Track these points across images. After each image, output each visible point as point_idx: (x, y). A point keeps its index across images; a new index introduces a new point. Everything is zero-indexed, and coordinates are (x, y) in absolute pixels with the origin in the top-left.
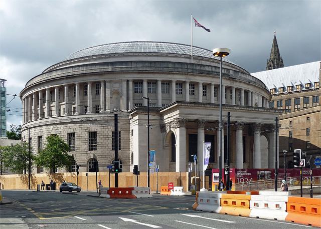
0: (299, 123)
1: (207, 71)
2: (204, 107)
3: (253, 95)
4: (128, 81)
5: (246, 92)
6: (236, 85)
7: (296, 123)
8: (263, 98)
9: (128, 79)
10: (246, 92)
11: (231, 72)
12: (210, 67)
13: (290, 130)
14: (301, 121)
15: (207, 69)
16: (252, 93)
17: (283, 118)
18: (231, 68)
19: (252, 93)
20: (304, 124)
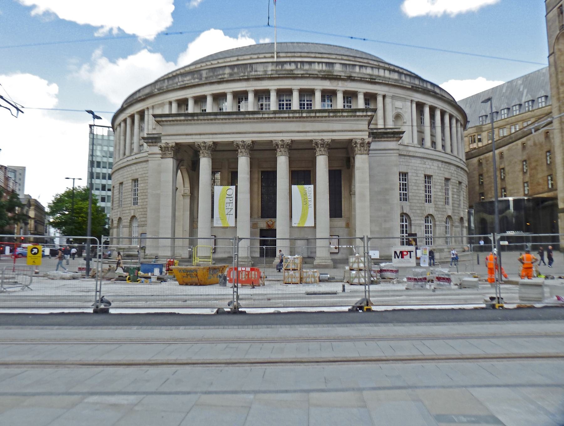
0: (535, 144)
1: (287, 70)
2: (198, 120)
3: (388, 100)
4: (170, 103)
5: (370, 98)
7: (531, 146)
8: (420, 106)
9: (171, 100)
10: (370, 98)
11: (338, 68)
12: (293, 64)
13: (525, 157)
14: (537, 142)
15: (287, 67)
16: (384, 97)
17: (514, 139)
18: (358, 63)
19: (384, 97)
20: (541, 145)
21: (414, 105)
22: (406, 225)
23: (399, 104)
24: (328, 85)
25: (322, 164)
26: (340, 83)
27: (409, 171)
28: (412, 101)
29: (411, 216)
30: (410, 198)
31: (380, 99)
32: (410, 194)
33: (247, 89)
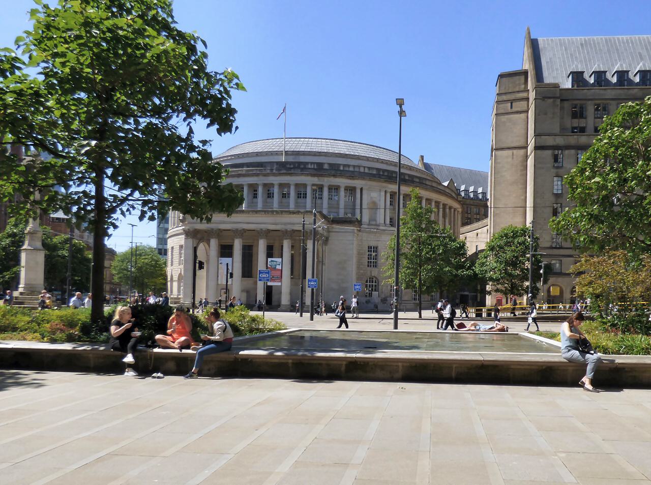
3: (364, 192)
6: (327, 181)
10: (351, 190)
16: (361, 189)
19: (361, 189)
21: (388, 196)
22: (375, 285)
23: (374, 195)
24: (316, 180)
25: (286, 245)
26: (326, 179)
27: (379, 245)
28: (386, 192)
29: (379, 278)
30: (379, 265)
31: (358, 192)
32: (379, 262)
33: (258, 183)
